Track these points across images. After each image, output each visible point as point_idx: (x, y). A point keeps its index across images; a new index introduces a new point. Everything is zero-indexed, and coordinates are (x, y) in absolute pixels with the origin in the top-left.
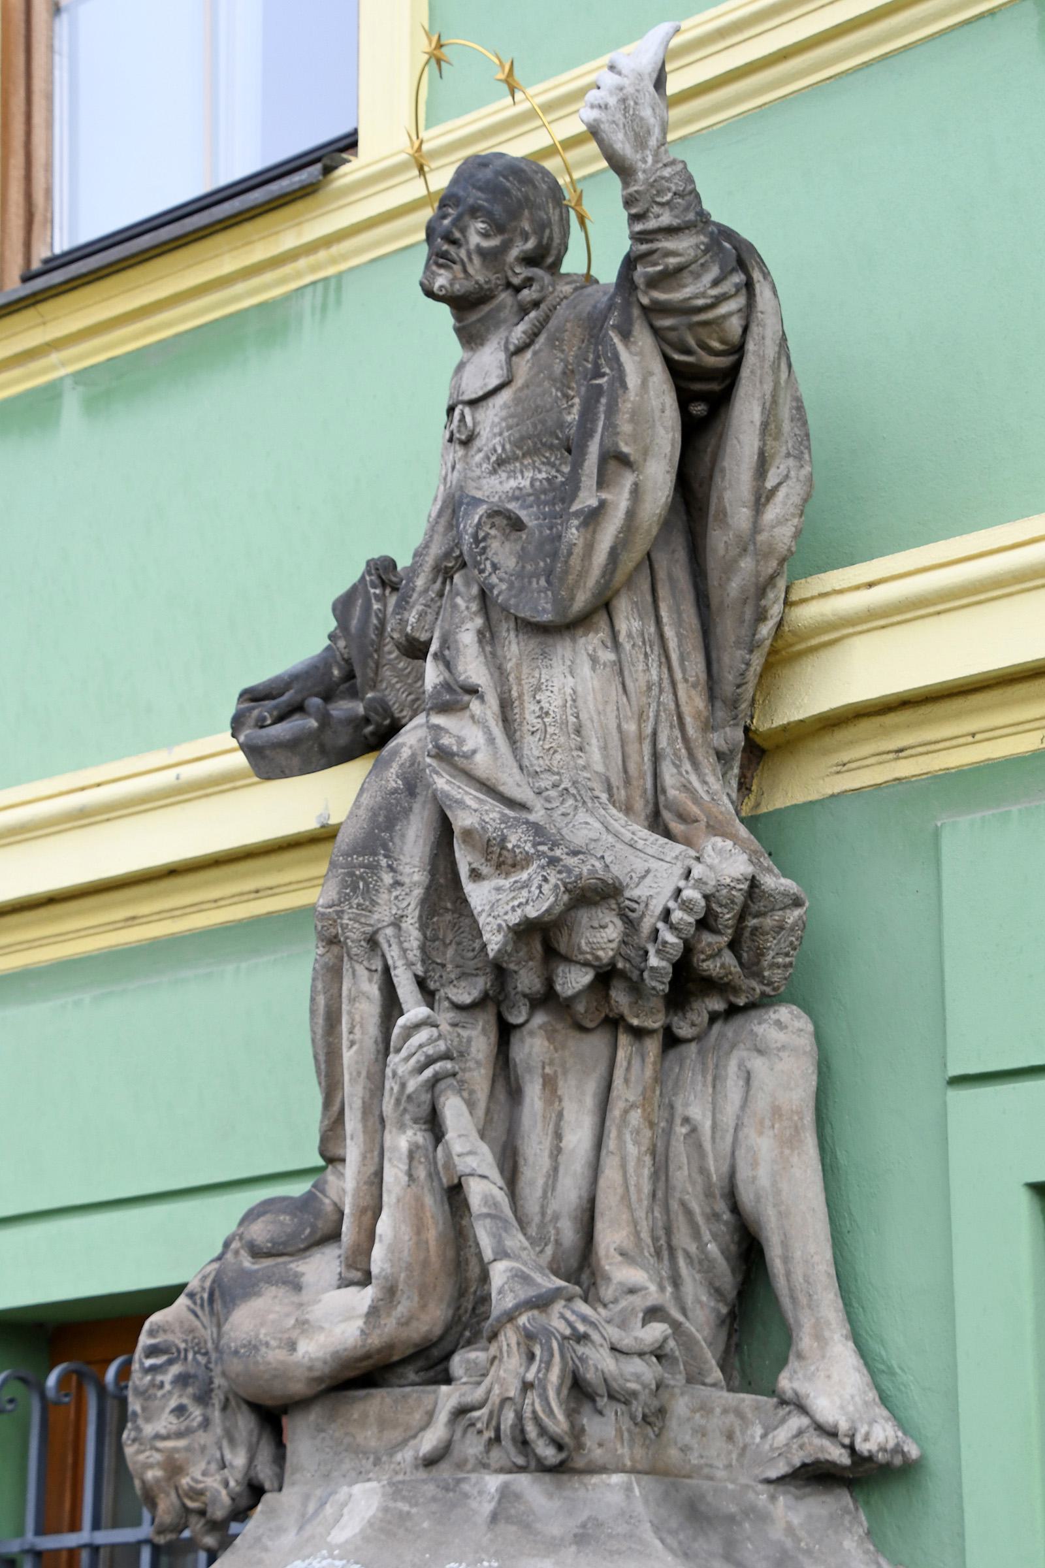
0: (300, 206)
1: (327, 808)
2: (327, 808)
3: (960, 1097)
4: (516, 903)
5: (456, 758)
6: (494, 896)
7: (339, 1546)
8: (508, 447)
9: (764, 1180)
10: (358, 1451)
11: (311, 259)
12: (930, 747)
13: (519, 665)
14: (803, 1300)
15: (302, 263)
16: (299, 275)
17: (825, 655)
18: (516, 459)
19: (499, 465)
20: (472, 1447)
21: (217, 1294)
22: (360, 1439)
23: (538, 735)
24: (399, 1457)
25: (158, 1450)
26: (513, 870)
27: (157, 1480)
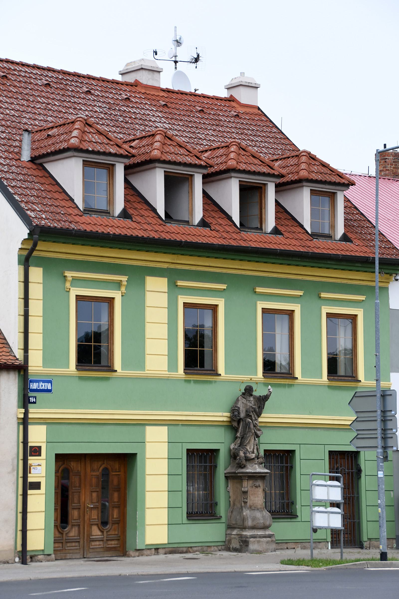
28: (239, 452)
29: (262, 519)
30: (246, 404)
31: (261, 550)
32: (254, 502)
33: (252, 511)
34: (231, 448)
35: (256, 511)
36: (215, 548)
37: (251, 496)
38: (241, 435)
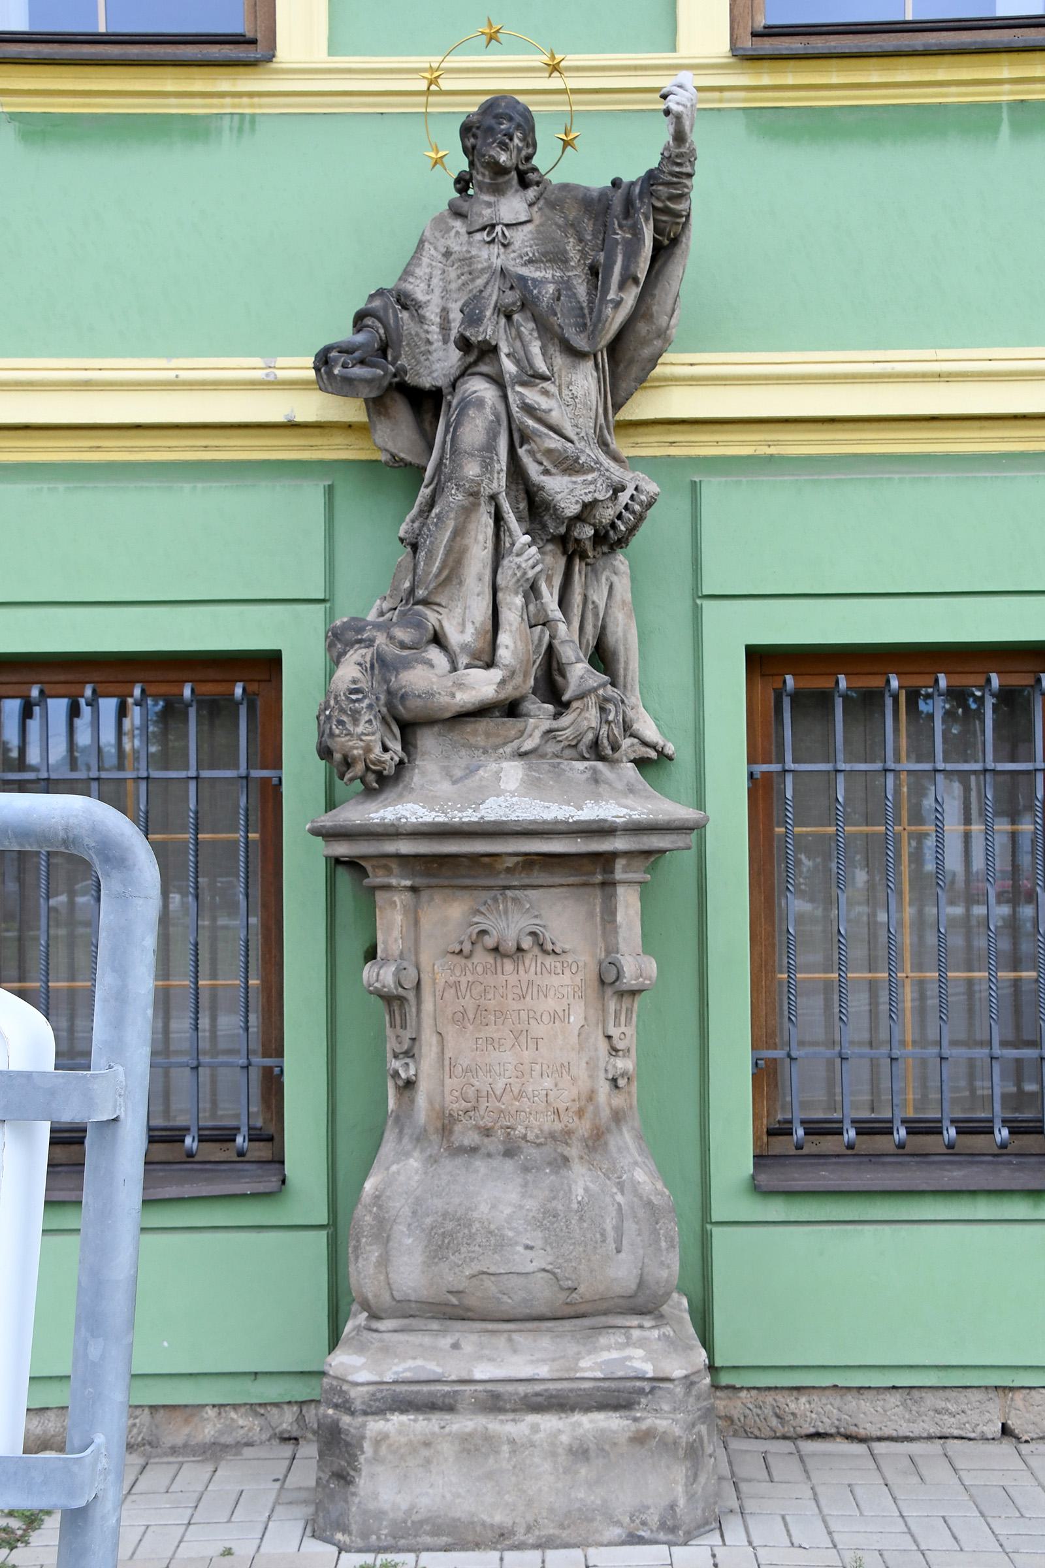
0: (241, 69)
1: (292, 411)
2: (292, 411)
3: (707, 605)
4: (587, 491)
6: (571, 486)
7: (516, 791)
8: (536, 254)
9: (620, 634)
10: (471, 747)
11: (237, 100)
12: (691, 444)
13: (560, 370)
14: (629, 687)
15: (228, 100)
16: (222, 106)
17: (650, 392)
18: (543, 262)
20: (551, 748)
21: (376, 665)
23: (571, 407)
24: (501, 750)
25: (361, 740)
27: (360, 755)
29: (535, 1237)
30: (467, 260)
31: (499, 1518)
32: (481, 1082)
33: (449, 1165)
35: (479, 1164)
36: (241, 1420)
37: (450, 1032)
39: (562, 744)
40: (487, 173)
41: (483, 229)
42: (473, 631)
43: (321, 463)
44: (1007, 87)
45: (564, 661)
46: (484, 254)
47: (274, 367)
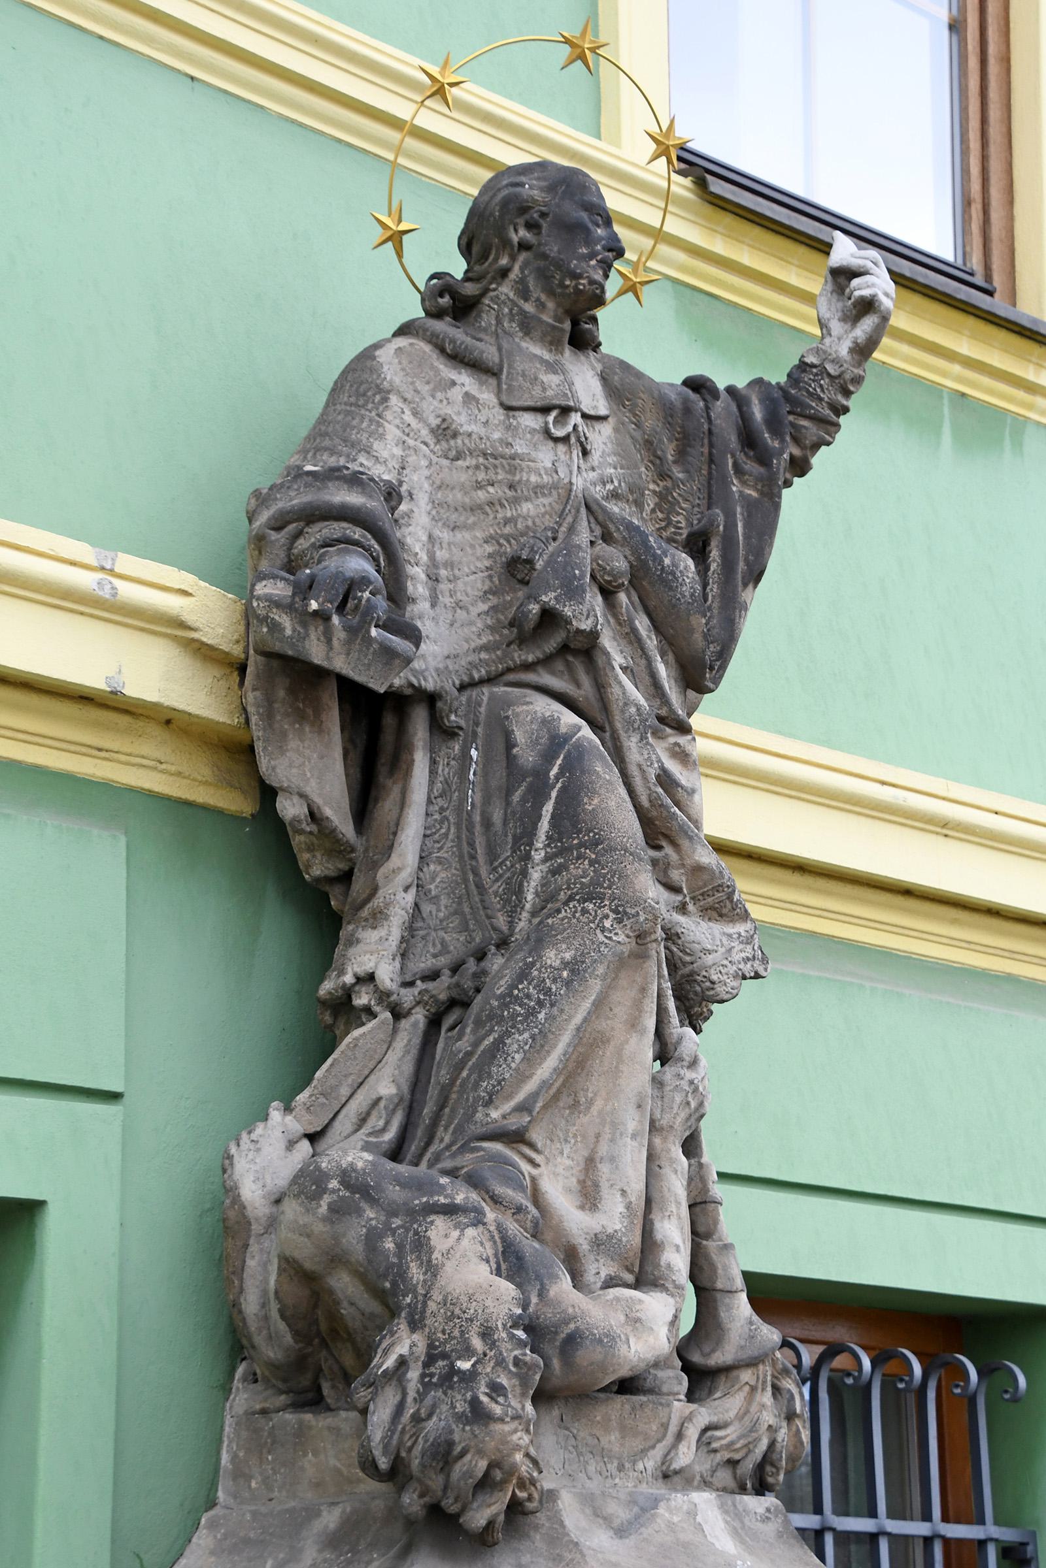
5: (679, 789)
10: (603, 1454)
19: (612, 495)
22: (604, 1441)
24: (640, 1466)
26: (718, 918)
28: (421, 1245)
34: (252, 1192)
38: (423, 962)
39: (718, 1457)
40: (551, 305)
41: (545, 410)
42: (621, 1208)
43: (107, 788)
44: (957, 368)
45: (719, 1285)
46: (545, 456)
47: (111, 572)
